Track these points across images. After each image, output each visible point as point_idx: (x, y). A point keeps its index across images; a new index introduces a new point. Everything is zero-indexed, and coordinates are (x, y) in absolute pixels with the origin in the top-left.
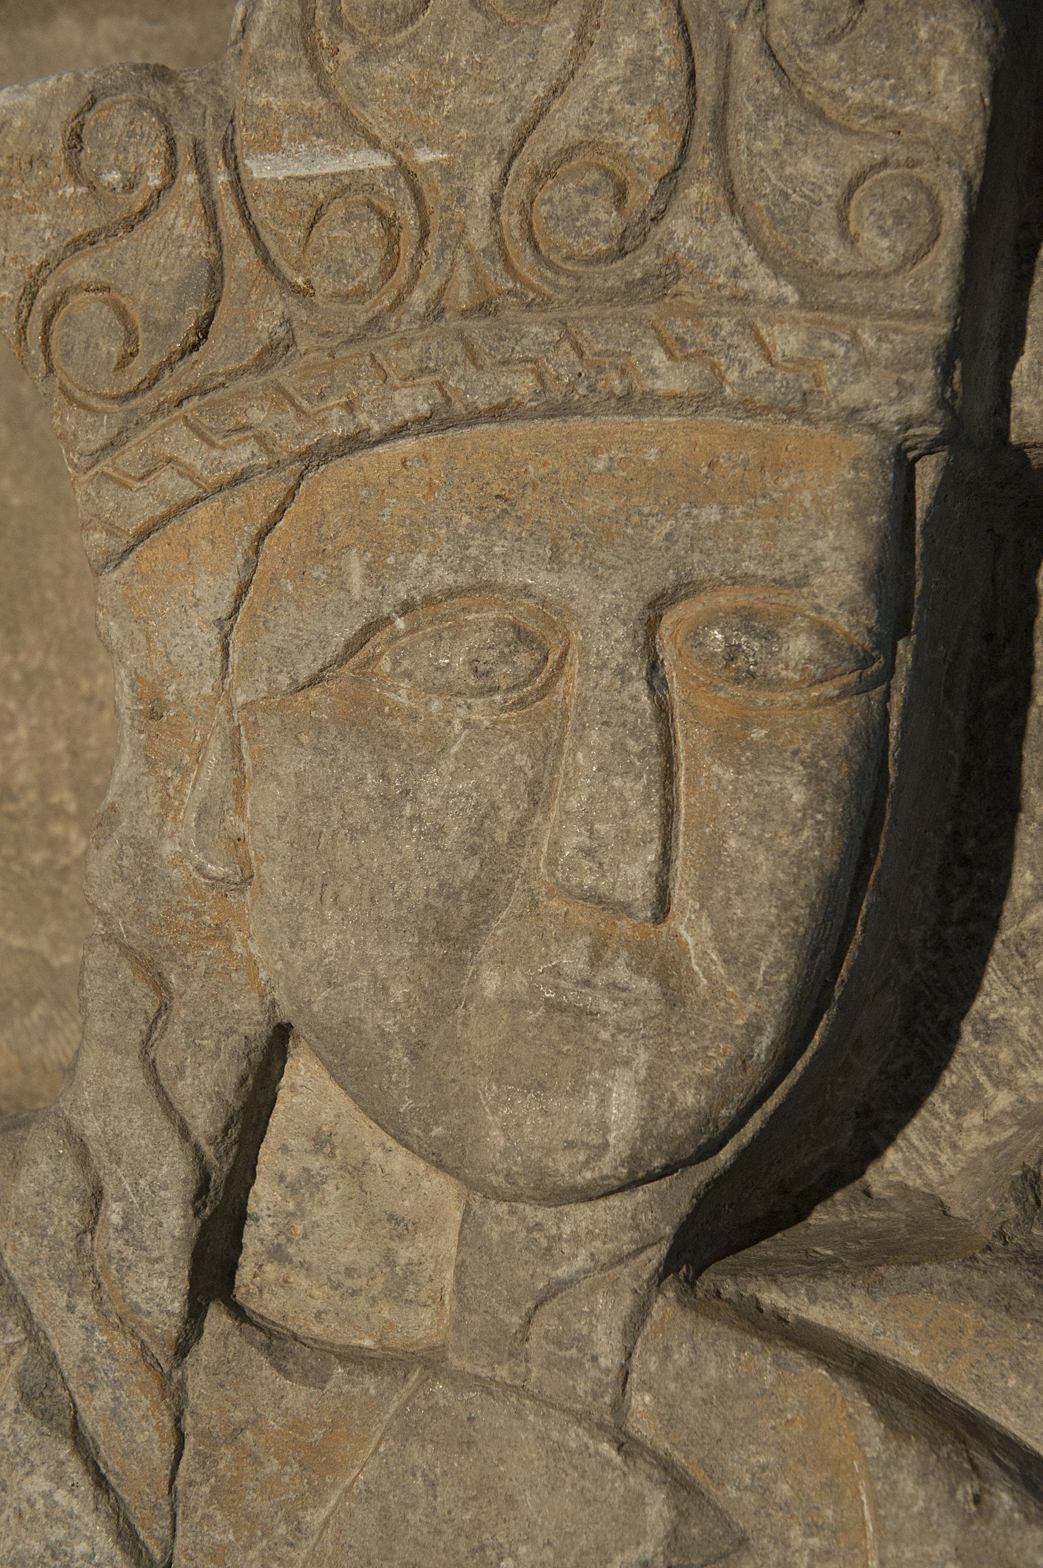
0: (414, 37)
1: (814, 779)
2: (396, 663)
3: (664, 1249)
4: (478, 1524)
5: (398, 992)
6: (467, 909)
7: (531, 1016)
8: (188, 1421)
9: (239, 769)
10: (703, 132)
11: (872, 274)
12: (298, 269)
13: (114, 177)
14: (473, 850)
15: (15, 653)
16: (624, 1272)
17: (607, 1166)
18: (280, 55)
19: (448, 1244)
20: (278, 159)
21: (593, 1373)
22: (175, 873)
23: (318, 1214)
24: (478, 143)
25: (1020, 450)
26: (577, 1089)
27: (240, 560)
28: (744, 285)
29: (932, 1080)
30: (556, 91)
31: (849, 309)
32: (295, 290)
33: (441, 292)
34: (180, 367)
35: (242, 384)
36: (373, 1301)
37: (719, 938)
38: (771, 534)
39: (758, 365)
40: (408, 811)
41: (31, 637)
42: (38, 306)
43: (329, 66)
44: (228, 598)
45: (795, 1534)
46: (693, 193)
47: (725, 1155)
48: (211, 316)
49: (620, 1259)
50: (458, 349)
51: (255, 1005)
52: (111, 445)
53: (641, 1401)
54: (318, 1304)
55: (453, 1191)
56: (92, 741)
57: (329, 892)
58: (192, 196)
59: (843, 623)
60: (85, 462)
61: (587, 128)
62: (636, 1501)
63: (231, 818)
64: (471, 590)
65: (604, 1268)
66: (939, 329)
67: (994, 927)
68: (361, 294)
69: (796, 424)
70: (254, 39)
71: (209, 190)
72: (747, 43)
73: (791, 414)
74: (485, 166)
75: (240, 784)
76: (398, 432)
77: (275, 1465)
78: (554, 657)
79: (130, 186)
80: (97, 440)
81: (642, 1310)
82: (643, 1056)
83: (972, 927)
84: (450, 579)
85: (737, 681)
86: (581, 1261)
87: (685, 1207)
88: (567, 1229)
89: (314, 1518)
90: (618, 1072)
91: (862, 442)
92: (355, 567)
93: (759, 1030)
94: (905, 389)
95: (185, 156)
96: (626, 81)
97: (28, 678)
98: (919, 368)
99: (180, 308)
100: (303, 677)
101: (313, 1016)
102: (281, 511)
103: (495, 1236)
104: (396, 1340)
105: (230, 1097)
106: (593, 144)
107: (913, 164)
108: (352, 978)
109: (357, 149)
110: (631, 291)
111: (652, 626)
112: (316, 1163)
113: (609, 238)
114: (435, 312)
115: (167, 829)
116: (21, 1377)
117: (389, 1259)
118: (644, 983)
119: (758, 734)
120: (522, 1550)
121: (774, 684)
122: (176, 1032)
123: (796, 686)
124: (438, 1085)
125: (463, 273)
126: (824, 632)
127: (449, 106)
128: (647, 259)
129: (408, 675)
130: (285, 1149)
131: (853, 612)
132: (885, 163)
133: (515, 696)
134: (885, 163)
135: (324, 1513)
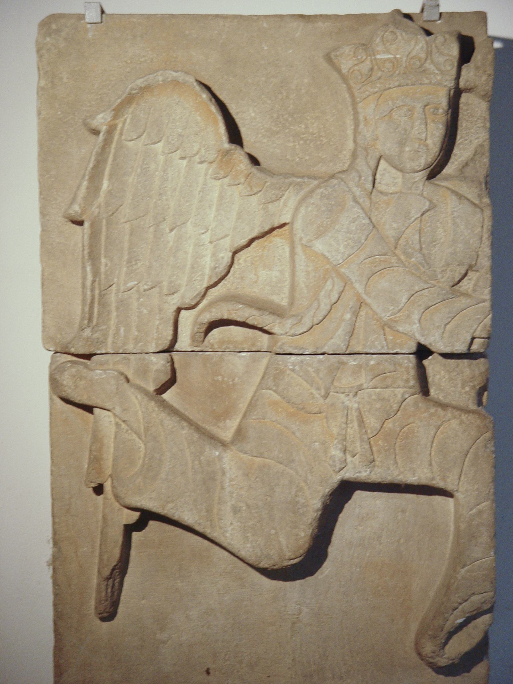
14: (405, 134)
17: (421, 168)
25: (460, 88)
35: (375, 82)
52: (360, 89)
64: (404, 105)
66: (454, 77)
72: (433, 45)
80: (358, 88)
89: (387, 210)
91: (446, 89)
121: (438, 115)
122: (369, 157)
126: (443, 109)
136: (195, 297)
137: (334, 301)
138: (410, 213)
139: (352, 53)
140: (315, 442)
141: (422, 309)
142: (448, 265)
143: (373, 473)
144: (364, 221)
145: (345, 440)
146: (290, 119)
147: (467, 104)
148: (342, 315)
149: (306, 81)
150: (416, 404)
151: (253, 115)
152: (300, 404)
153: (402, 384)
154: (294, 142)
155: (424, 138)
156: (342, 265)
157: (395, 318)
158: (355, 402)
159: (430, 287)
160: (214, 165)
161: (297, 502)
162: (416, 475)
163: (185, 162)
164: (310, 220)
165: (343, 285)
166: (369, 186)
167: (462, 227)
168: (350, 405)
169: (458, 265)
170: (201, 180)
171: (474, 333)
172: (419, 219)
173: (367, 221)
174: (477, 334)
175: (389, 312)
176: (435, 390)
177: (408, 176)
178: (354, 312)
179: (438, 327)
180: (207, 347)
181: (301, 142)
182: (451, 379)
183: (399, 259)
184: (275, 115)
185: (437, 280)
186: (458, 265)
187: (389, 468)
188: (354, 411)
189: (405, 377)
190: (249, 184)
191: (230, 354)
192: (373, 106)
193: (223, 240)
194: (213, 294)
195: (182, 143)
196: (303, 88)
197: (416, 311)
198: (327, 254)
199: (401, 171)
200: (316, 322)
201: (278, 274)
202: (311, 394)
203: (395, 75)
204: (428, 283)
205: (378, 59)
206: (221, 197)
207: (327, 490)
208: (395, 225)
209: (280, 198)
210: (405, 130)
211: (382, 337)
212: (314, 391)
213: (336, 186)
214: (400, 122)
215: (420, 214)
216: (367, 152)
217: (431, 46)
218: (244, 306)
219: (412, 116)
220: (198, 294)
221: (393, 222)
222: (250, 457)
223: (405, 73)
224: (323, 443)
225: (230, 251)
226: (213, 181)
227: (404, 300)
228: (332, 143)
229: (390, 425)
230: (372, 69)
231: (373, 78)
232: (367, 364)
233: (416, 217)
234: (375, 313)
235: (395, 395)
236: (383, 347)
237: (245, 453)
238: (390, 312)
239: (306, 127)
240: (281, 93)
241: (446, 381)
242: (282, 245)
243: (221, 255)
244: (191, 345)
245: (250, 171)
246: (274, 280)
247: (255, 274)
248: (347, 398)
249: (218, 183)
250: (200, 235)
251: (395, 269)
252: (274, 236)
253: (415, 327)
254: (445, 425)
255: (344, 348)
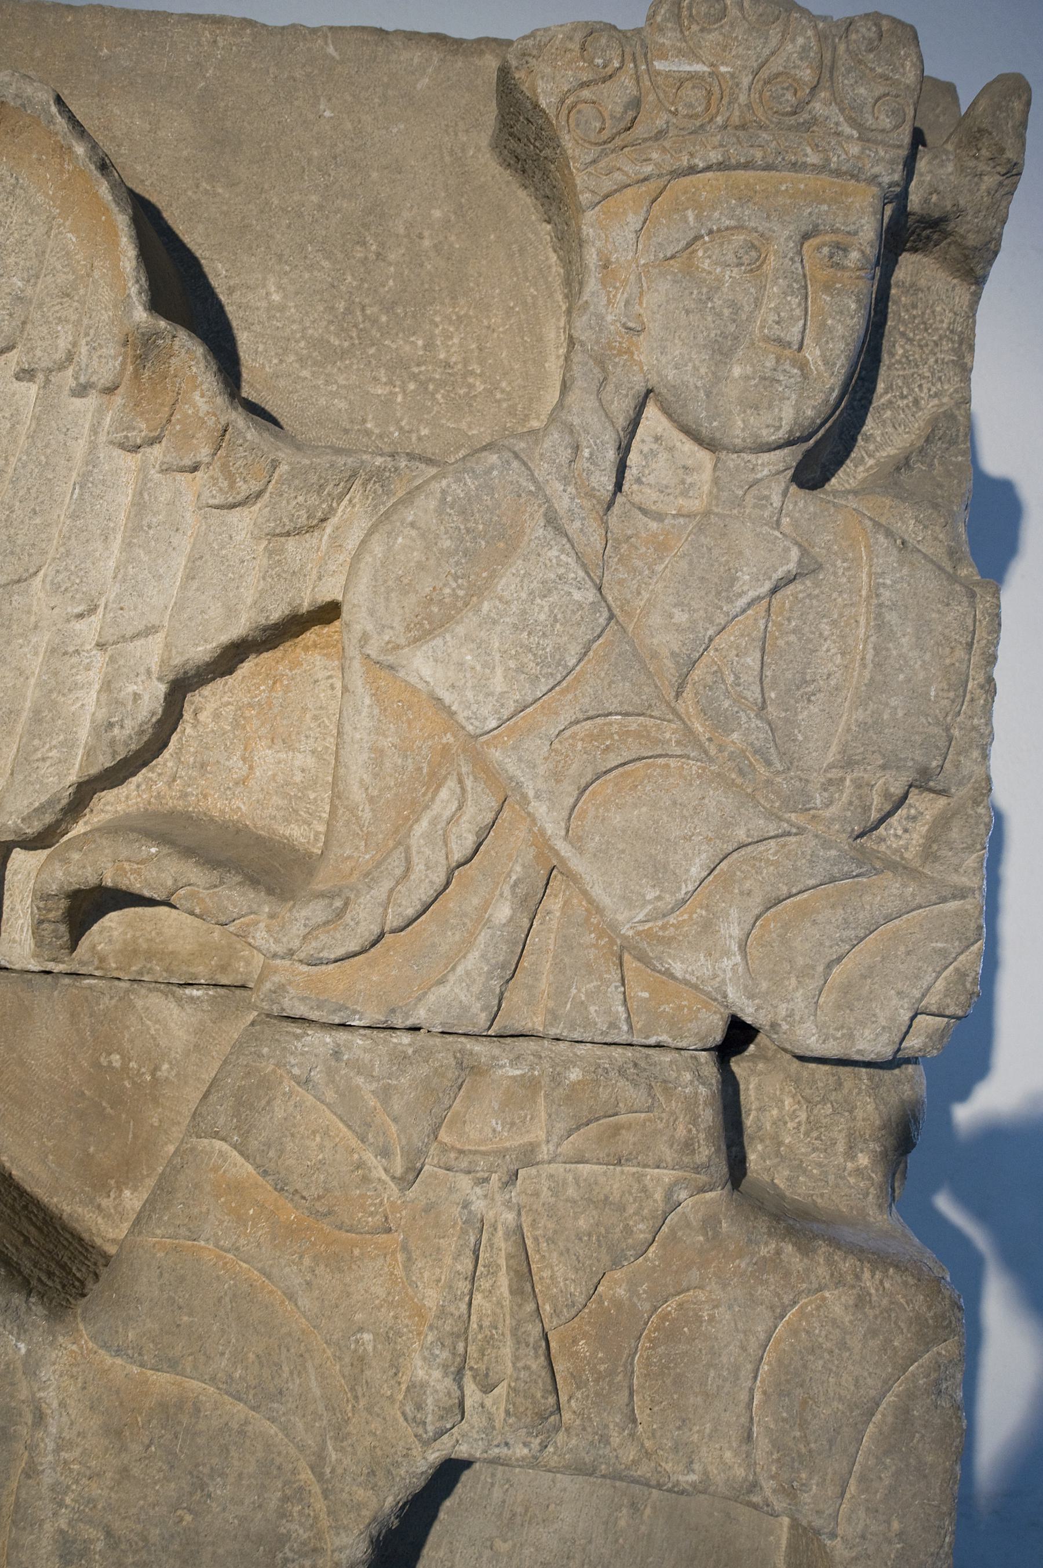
0: (722, 26)
1: (858, 301)
2: (705, 252)
3: (793, 470)
4: (727, 562)
5: (703, 371)
6: (730, 343)
7: (753, 382)
8: (609, 534)
9: (641, 287)
10: (826, 75)
11: (883, 131)
12: (672, 104)
13: (600, 61)
14: (734, 321)
15: (454, 308)
16: (781, 477)
17: (781, 434)
18: (669, 25)
19: (707, 475)
20: (667, 63)
21: (770, 509)
22: (612, 327)
23: (654, 466)
24: (745, 67)
26: (770, 407)
27: (645, 209)
28: (840, 129)
29: (847, 456)
30: (773, 54)
31: (876, 142)
32: (670, 111)
33: (728, 118)
34: (623, 136)
35: (648, 144)
36: (676, 497)
37: (823, 357)
38: (846, 216)
39: (844, 156)
40: (710, 305)
41: (462, 301)
42: (565, 106)
43: (687, 33)
44: (641, 223)
45: (839, 563)
46: (823, 95)
47: (812, 442)
48: (636, 118)
49: (779, 473)
50: (735, 140)
51: (642, 379)
52: (594, 162)
53: (785, 521)
54: (655, 499)
55: (708, 457)
56: (488, 345)
57: (677, 334)
58: (632, 72)
59: (868, 251)
60: (583, 167)
61: (785, 67)
62: (786, 550)
63: (637, 307)
64: (736, 227)
65: (774, 475)
67: (870, 403)
68: (696, 116)
69: (853, 181)
70: (659, 19)
71: (637, 72)
72: (842, 48)
73: (852, 176)
74: (747, 75)
75: (641, 293)
76: (708, 168)
77: (643, 550)
78: (763, 256)
79: (605, 67)
80: (589, 159)
81: (787, 489)
82: (794, 396)
83: (863, 402)
84: (728, 222)
85: (832, 267)
86: (766, 472)
87: (800, 457)
88: (760, 462)
89: (659, 568)
90: (786, 402)
92: (690, 215)
93: (834, 390)
94: (894, 171)
95: (628, 57)
96: (799, 53)
97: (460, 318)
98: (898, 164)
99: (625, 112)
100: (669, 255)
101: (668, 381)
102: (661, 193)
103: (732, 466)
104: (685, 511)
105: (631, 412)
106: (787, 74)
107: (897, 96)
108: (686, 366)
109: (698, 63)
110: (797, 128)
111: (802, 244)
112: (655, 446)
113: (792, 106)
114: (725, 127)
115: (610, 310)
116: (545, 515)
117: (683, 482)
118: (796, 371)
119: (838, 286)
120: (745, 569)
121: (844, 268)
122: (610, 387)
123: (852, 270)
124: (716, 407)
125: (737, 113)
126: (863, 252)
127: (734, 53)
128: (805, 116)
129: (710, 257)
130: (643, 441)
131: (871, 247)
132: (888, 94)
133: (749, 268)
134: (888, 94)
135: (663, 566)
136: (41, 810)
137: (457, 856)
138: (733, 580)
139: (575, 46)
140: (361, 1330)
141: (755, 904)
142: (848, 763)
143: (550, 1449)
144: (577, 596)
145: (464, 1334)
146: (384, 319)
147: (913, 288)
148: (486, 905)
149: (437, 214)
150: (710, 1223)
151: (276, 297)
152: (319, 1198)
153: (669, 1155)
154: (391, 383)
155: (796, 339)
156: (495, 737)
157: (664, 928)
158: (508, 1204)
159: (789, 834)
160: (118, 400)
161: (283, 1540)
162: (696, 1466)
163: (32, 390)
164: (399, 579)
165: (495, 805)
166: (605, 482)
167: (903, 640)
168: (490, 1215)
169: (883, 767)
170: (79, 449)
171: (924, 996)
172: (764, 603)
173: (591, 595)
174: (932, 1001)
175: (643, 906)
176: (763, 1157)
177: (732, 460)
178: (525, 899)
179: (805, 973)
180: (82, 963)
181: (412, 386)
182: (813, 1124)
183: (689, 731)
184: (341, 306)
185: (810, 809)
186: (883, 767)
187: (605, 1440)
188: (500, 1233)
189: (681, 1132)
190: (225, 468)
191: (150, 990)
192: (634, 221)
193: (140, 642)
194: (108, 808)
195: (24, 323)
196: (426, 233)
197: (734, 913)
198: (447, 697)
199: (710, 444)
200: (393, 920)
201: (310, 761)
202: (360, 1165)
203: (711, 128)
204: (780, 819)
205: (658, 73)
206: (139, 506)
207: (390, 1501)
208: (681, 617)
209: (323, 520)
210: (735, 306)
211: (614, 993)
212: (370, 1157)
213: (495, 473)
214: (720, 280)
215: (768, 586)
216: (604, 369)
217: (835, 49)
218: (166, 850)
219: (761, 266)
220: (50, 803)
221: (675, 606)
222: (136, 1369)
223: (743, 127)
224: (389, 1337)
225: (160, 679)
226: (117, 452)
227: (696, 871)
228: (498, 396)
229: (621, 1292)
230: (636, 103)
231: (640, 130)
232: (556, 1079)
233: (752, 594)
234: (595, 908)
235: (644, 1190)
236: (613, 1025)
237: (118, 1352)
238: (650, 907)
239: (429, 346)
240: (364, 244)
241: (797, 1128)
242: (330, 677)
243: (132, 688)
244: (35, 956)
245: (223, 421)
246: (298, 778)
247: (244, 759)
248: (478, 1190)
249: (130, 461)
250: (68, 621)
251: (673, 763)
252: (306, 649)
253: (727, 963)
254: (807, 1304)
255: (483, 1019)
